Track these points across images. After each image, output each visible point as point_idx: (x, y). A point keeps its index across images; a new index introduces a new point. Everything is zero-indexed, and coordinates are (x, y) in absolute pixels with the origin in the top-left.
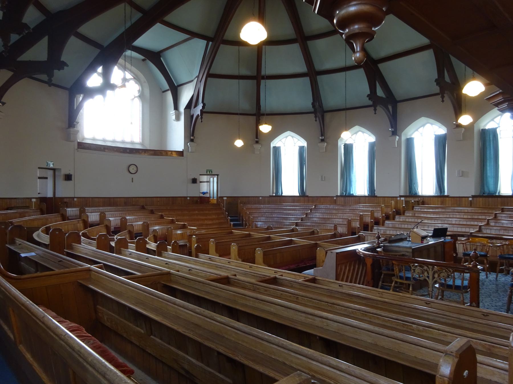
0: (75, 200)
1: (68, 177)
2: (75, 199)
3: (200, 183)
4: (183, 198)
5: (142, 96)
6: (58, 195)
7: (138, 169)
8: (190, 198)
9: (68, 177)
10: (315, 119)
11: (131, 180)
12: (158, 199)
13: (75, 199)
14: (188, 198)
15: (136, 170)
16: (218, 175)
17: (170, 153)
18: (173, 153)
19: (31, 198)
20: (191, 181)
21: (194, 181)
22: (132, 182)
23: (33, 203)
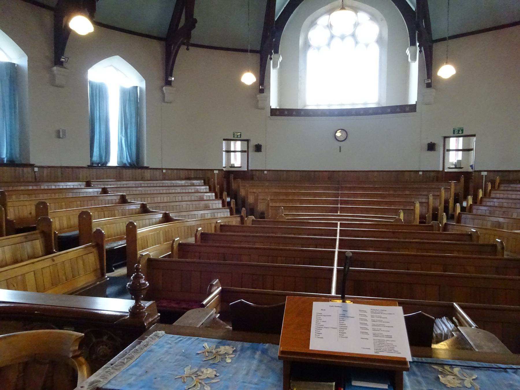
1: (258, 148)
2: (266, 172)
4: (412, 173)
5: (380, 40)
6: (250, 168)
7: (348, 134)
8: (424, 173)
9: (258, 148)
11: (339, 149)
12: (376, 174)
13: (266, 172)
14: (421, 173)
15: (345, 137)
16: (445, 138)
19: (213, 170)
20: (426, 147)
21: (431, 147)
22: (340, 151)
23: (216, 174)
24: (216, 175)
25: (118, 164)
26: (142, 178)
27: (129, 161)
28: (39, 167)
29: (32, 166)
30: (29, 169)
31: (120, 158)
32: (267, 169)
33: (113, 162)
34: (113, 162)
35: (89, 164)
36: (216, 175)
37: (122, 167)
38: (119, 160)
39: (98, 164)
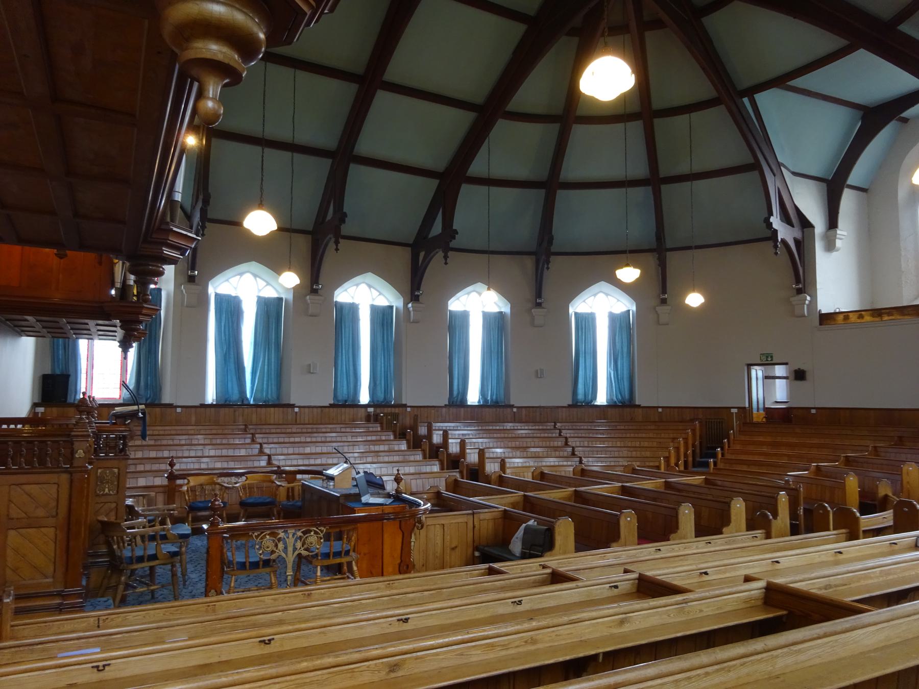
0: (812, 412)
3: (788, 375)
10: (444, 261)
17: (841, 317)
18: (851, 315)
24: (734, 415)
25: (607, 402)
26: (631, 419)
27: (620, 397)
28: (517, 407)
29: (512, 406)
30: (509, 410)
31: (610, 395)
32: (816, 406)
33: (602, 399)
34: (602, 399)
35: (570, 403)
36: (734, 415)
37: (611, 406)
38: (609, 398)
39: (582, 403)
